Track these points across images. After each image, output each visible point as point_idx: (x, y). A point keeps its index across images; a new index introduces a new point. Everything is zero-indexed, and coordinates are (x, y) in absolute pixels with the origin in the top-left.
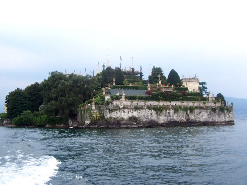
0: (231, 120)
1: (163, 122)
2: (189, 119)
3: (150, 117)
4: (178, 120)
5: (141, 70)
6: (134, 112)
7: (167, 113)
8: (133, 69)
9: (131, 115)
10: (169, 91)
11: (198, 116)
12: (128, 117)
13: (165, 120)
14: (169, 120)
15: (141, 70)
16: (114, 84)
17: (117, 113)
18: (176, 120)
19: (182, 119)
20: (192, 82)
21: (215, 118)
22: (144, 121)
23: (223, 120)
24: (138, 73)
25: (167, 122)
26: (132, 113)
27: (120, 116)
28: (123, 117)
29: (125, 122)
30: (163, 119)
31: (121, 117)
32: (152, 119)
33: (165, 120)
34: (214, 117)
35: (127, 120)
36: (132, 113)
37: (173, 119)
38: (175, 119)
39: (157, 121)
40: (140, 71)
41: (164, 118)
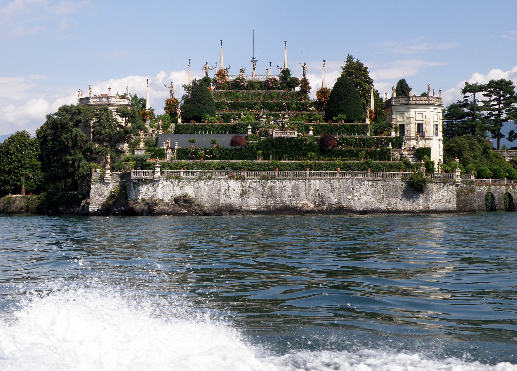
0: (444, 208)
1: (256, 209)
2: (323, 202)
3: (222, 199)
4: (293, 204)
5: (304, 75)
6: (186, 188)
7: (267, 189)
8: (286, 73)
9: (178, 193)
10: (289, 136)
11: (349, 197)
12: (172, 196)
13: (260, 205)
14: (269, 204)
15: (304, 75)
16: (180, 121)
17: (148, 189)
18: (288, 204)
19: (305, 202)
20: (416, 104)
21: (396, 203)
22: (209, 205)
23: (421, 208)
24: (294, 82)
25: (265, 209)
26: (182, 188)
27: (153, 196)
28: (160, 196)
29: (162, 208)
30: (257, 202)
31: (156, 198)
32: (229, 201)
33: (260, 205)
34: (392, 200)
35: (167, 203)
36: (182, 188)
37: (282, 201)
38: (285, 203)
39: (241, 207)
40: (301, 78)
41: (257, 199)
